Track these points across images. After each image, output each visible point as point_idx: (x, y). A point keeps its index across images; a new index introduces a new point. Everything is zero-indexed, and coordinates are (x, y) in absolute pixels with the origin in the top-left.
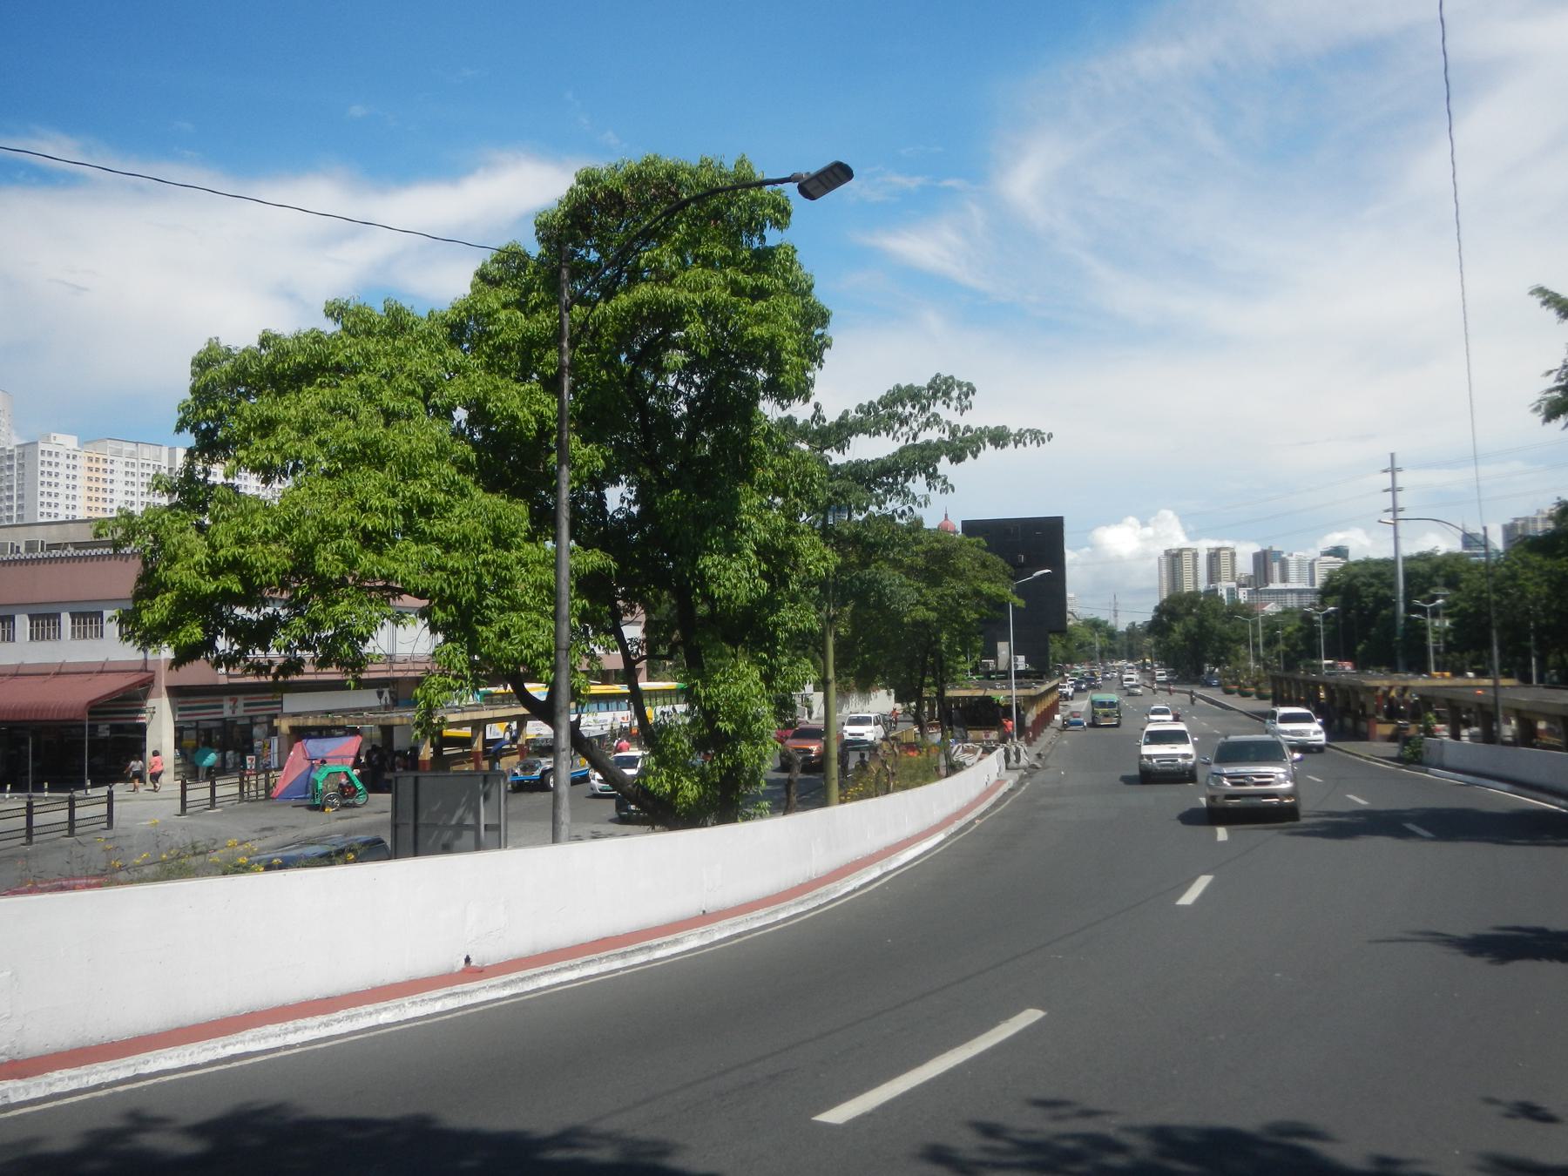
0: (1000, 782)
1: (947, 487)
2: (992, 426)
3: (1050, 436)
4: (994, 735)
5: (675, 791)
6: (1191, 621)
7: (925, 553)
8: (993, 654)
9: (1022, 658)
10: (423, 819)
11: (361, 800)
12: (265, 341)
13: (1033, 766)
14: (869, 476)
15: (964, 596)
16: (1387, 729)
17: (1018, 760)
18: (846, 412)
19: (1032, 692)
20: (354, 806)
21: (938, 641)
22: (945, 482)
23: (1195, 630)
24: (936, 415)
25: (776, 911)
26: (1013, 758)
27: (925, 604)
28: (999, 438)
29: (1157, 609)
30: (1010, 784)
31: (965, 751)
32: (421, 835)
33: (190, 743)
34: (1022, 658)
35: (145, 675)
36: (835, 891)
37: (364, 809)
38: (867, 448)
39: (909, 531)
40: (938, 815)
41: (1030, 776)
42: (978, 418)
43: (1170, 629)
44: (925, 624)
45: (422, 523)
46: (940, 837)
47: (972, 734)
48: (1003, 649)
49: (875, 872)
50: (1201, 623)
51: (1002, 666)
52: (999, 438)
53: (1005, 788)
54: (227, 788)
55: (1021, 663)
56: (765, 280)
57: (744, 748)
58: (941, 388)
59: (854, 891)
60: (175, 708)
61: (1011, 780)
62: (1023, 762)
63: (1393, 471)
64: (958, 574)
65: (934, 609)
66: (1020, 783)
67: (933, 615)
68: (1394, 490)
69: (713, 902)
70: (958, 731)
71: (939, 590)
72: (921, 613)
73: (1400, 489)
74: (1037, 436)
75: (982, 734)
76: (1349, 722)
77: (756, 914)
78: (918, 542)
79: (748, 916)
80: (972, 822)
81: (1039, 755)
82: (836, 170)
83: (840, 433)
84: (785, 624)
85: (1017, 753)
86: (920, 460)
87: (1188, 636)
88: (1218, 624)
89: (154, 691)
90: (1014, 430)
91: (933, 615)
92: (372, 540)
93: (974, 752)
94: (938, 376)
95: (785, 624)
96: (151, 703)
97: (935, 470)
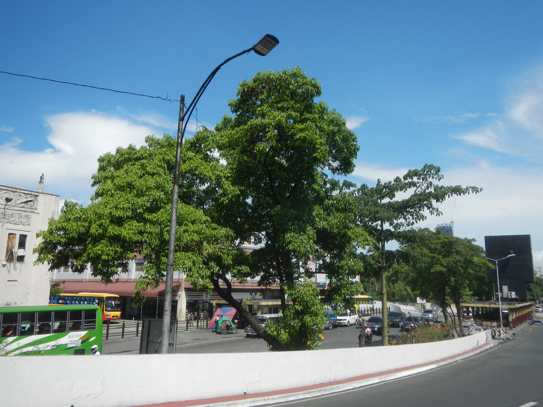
0: (486, 344)
1: (439, 214)
2: (454, 186)
3: (481, 189)
4: (495, 324)
5: (278, 335)
7: (441, 243)
9: (513, 293)
10: (150, 339)
11: (234, 331)
12: (118, 151)
13: (508, 339)
14: (402, 208)
15: (459, 262)
17: (500, 336)
18: (390, 182)
19: (512, 307)
20: (232, 333)
21: (450, 280)
22: (437, 210)
24: (431, 183)
25: (288, 396)
26: (497, 333)
27: (441, 264)
28: (457, 190)
30: (492, 345)
31: (476, 330)
32: (149, 346)
33: (192, 306)
35: (178, 284)
36: (337, 389)
37: (235, 335)
38: (401, 196)
39: (436, 234)
40: (438, 356)
41: (505, 341)
42: (446, 182)
44: (440, 272)
45: (146, 216)
46: (434, 366)
47: (485, 323)
49: (375, 380)
51: (505, 296)
52: (457, 190)
53: (488, 347)
54: (203, 323)
55: (513, 295)
56: (308, 116)
57: (308, 319)
58: (431, 170)
59: (354, 389)
60: (187, 296)
61: (493, 343)
62: (502, 336)
64: (458, 253)
65: (445, 267)
66: (498, 345)
67: (444, 270)
69: (251, 389)
70: (478, 321)
71: (447, 259)
72: (438, 268)
74: (476, 190)
75: (489, 323)
77: (271, 397)
78: (438, 238)
79: (266, 398)
80: (457, 361)
81: (514, 334)
82: (269, 39)
83: (390, 190)
84: (343, 266)
85: (499, 332)
86: (421, 201)
89: (180, 289)
90: (464, 187)
91: (444, 270)
92: (119, 221)
93: (480, 330)
94: (426, 165)
95: (343, 266)
96: (179, 293)
97: (431, 205)
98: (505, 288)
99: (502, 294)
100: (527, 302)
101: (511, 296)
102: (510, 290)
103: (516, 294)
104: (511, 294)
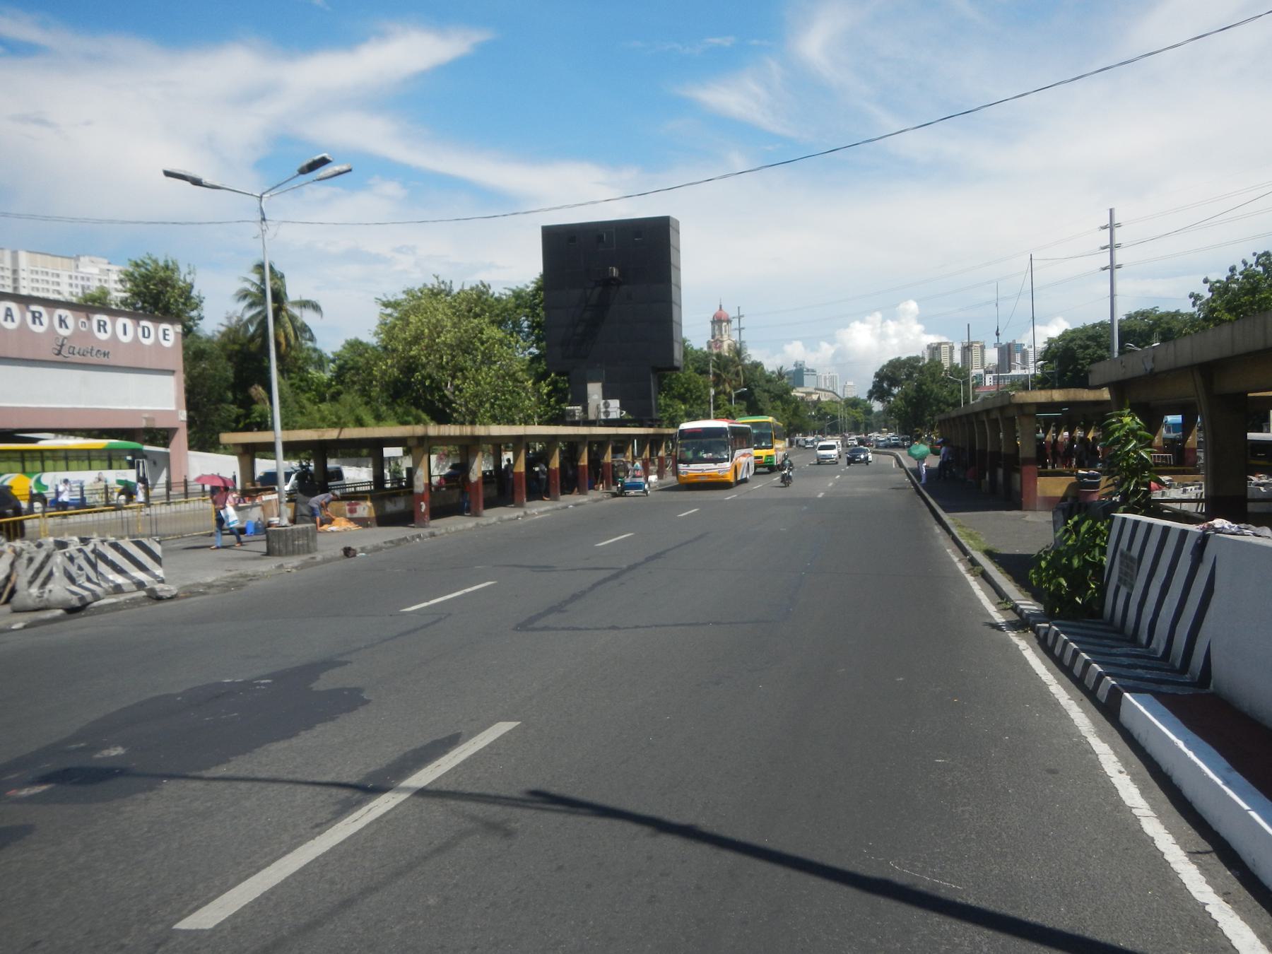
6: (909, 387)
8: (582, 399)
9: (615, 404)
16: (1054, 486)
23: (913, 394)
29: (877, 375)
34: (615, 404)
43: (889, 393)
48: (594, 391)
50: (919, 388)
51: (592, 417)
55: (615, 408)
63: (1112, 227)
68: (1112, 247)
73: (1118, 246)
76: (1000, 472)
81: (348, 552)
87: (905, 396)
88: (935, 388)
98: (594, 391)
99: (585, 410)
100: (651, 426)
101: (607, 413)
102: (607, 395)
103: (622, 407)
104: (606, 405)
